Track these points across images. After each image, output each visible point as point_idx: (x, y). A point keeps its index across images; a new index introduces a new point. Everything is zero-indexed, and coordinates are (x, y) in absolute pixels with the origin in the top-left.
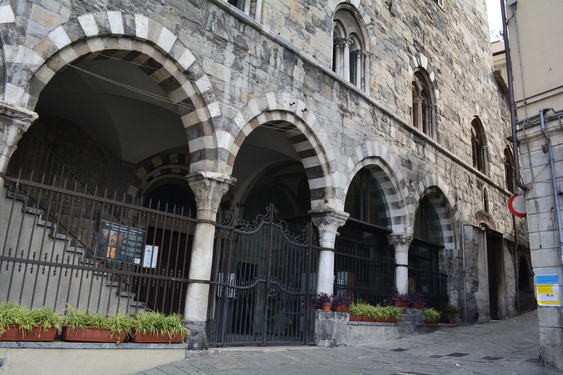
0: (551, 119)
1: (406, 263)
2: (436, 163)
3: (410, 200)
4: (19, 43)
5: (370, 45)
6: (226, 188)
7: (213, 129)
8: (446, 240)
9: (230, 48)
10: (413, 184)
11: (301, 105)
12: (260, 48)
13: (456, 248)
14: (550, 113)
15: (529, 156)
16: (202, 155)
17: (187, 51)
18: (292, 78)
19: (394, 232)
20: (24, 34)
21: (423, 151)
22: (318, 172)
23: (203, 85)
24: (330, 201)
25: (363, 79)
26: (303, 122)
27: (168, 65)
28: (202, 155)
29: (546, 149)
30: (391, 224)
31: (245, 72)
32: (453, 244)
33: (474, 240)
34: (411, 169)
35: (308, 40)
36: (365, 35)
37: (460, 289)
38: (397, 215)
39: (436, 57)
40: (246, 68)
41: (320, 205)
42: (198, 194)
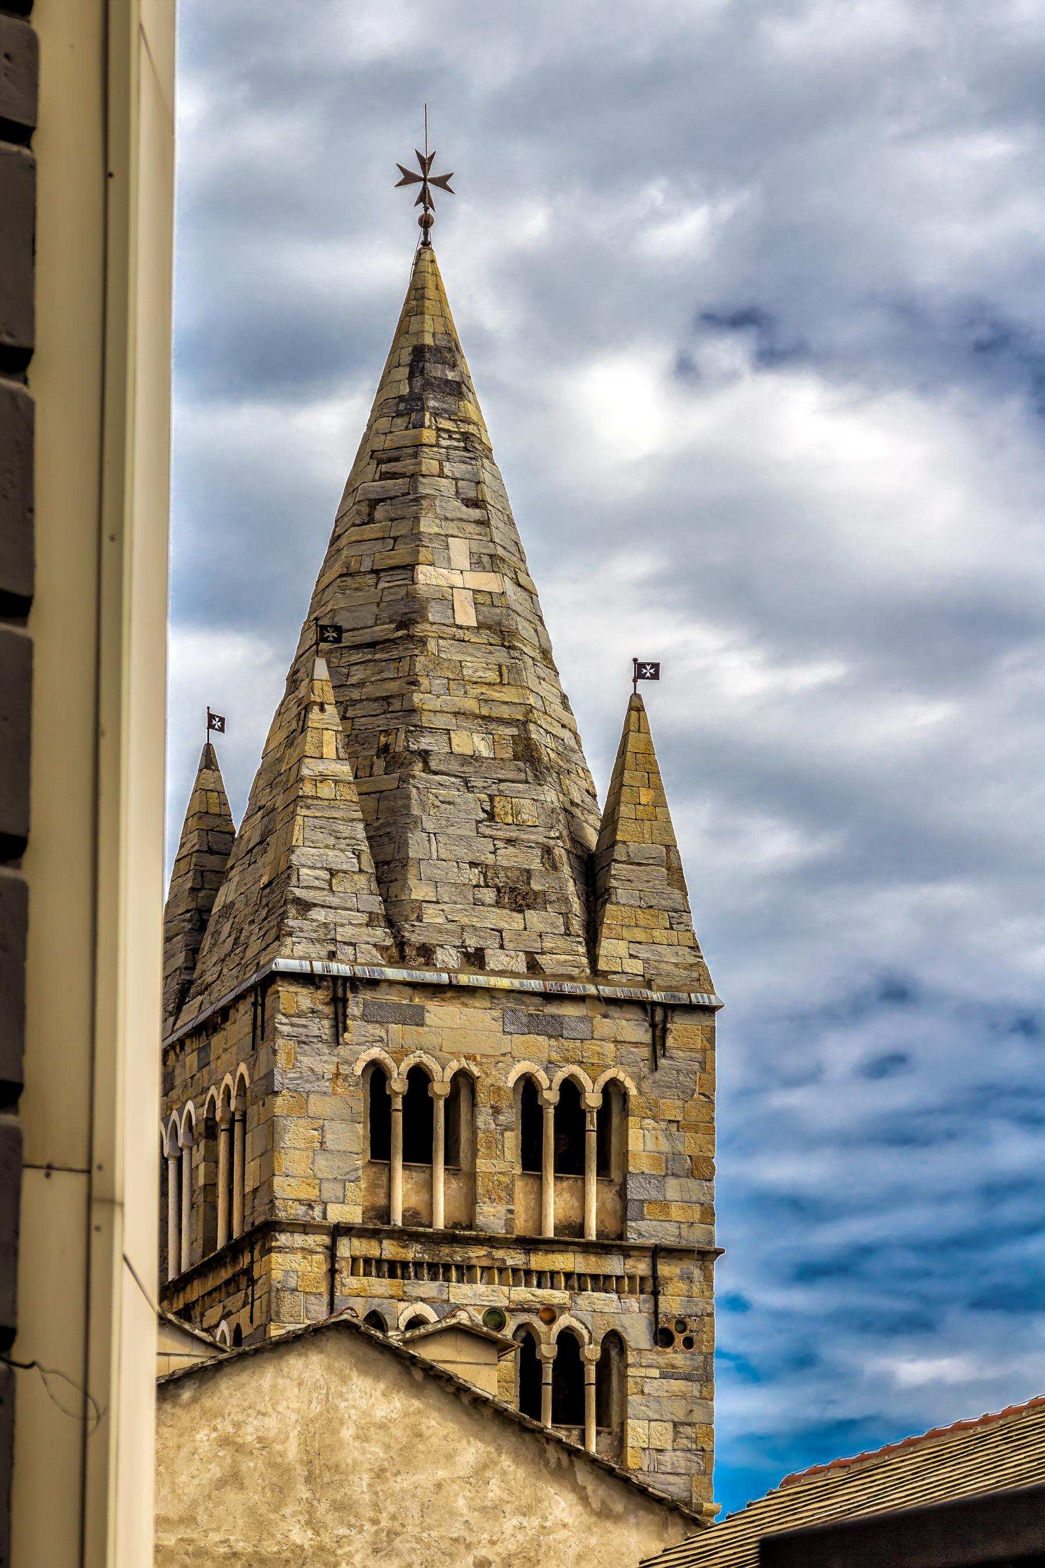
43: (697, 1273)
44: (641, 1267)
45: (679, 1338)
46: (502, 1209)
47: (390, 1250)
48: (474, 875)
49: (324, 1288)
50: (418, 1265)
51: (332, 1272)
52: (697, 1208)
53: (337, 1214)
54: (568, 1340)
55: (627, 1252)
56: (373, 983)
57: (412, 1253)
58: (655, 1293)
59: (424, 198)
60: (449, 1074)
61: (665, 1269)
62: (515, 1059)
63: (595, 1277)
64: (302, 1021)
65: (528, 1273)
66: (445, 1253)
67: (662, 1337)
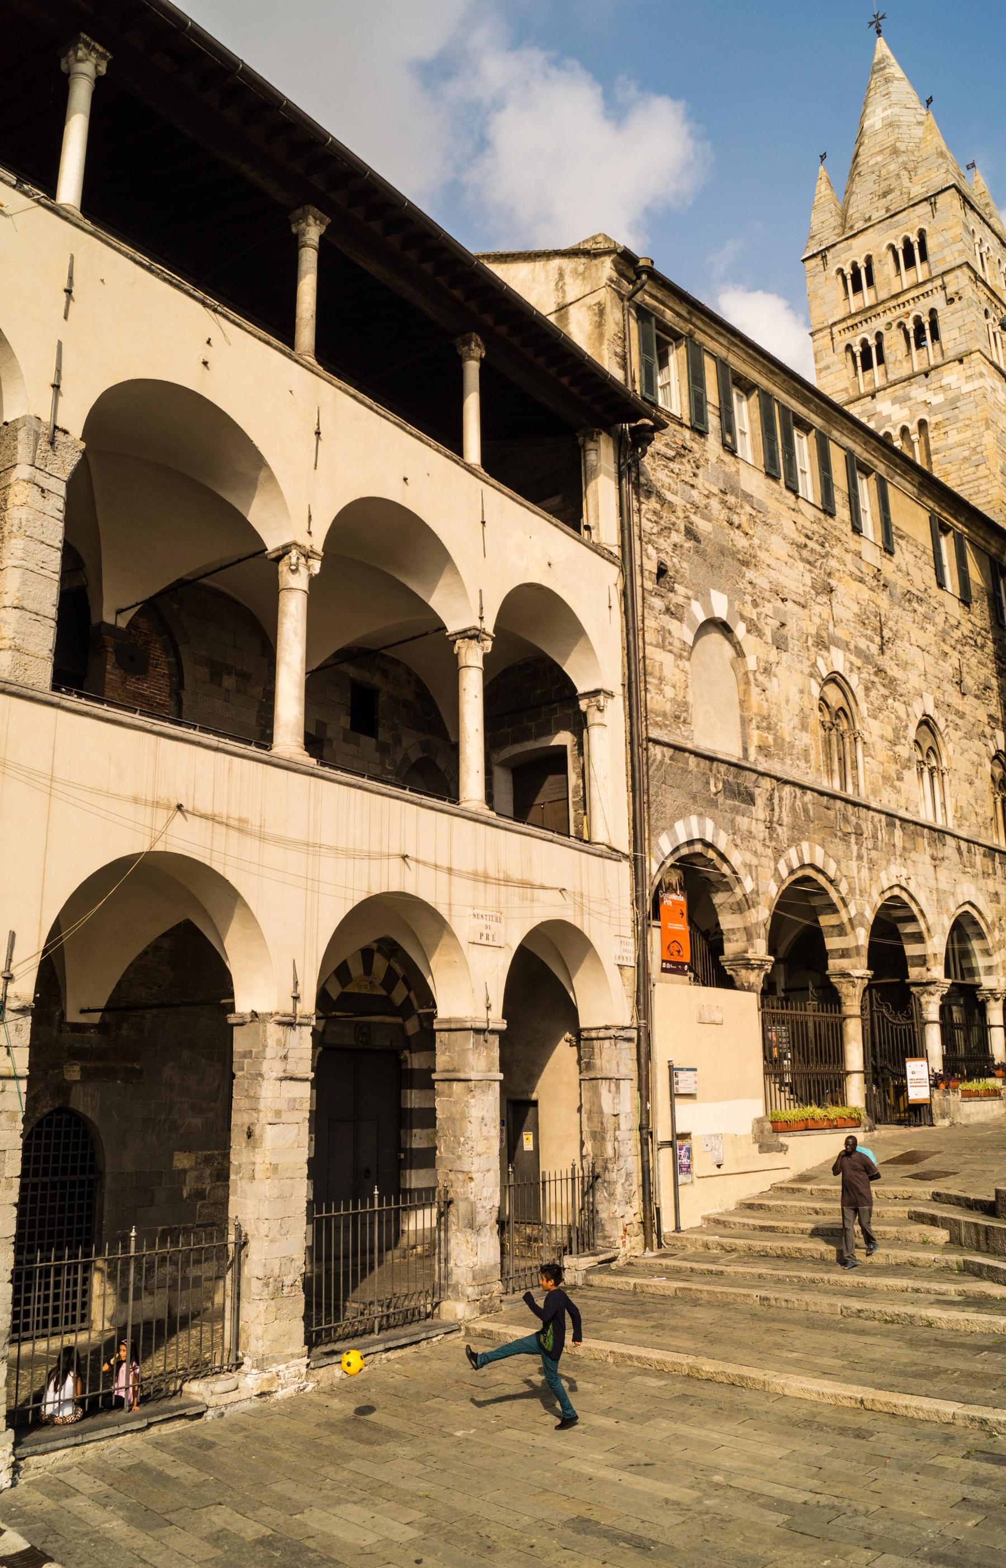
1: (1002, 1023)
4: (759, 904)
6: (866, 981)
7: (853, 928)
11: (904, 872)
12: (870, 826)
16: (844, 954)
17: (831, 860)
18: (894, 845)
20: (758, 895)
22: (919, 938)
23: (844, 887)
24: (933, 969)
26: (905, 890)
27: (821, 880)
28: (844, 954)
31: (865, 859)
34: (999, 903)
35: (899, 792)
36: (941, 745)
38: (987, 964)
40: (865, 855)
41: (920, 973)
44: (938, 282)
45: (956, 299)
46: (886, 290)
47: (850, 322)
50: (861, 322)
51: (832, 339)
54: (917, 320)
55: (930, 280)
56: (834, 245)
57: (858, 319)
61: (947, 279)
63: (923, 295)
66: (869, 314)
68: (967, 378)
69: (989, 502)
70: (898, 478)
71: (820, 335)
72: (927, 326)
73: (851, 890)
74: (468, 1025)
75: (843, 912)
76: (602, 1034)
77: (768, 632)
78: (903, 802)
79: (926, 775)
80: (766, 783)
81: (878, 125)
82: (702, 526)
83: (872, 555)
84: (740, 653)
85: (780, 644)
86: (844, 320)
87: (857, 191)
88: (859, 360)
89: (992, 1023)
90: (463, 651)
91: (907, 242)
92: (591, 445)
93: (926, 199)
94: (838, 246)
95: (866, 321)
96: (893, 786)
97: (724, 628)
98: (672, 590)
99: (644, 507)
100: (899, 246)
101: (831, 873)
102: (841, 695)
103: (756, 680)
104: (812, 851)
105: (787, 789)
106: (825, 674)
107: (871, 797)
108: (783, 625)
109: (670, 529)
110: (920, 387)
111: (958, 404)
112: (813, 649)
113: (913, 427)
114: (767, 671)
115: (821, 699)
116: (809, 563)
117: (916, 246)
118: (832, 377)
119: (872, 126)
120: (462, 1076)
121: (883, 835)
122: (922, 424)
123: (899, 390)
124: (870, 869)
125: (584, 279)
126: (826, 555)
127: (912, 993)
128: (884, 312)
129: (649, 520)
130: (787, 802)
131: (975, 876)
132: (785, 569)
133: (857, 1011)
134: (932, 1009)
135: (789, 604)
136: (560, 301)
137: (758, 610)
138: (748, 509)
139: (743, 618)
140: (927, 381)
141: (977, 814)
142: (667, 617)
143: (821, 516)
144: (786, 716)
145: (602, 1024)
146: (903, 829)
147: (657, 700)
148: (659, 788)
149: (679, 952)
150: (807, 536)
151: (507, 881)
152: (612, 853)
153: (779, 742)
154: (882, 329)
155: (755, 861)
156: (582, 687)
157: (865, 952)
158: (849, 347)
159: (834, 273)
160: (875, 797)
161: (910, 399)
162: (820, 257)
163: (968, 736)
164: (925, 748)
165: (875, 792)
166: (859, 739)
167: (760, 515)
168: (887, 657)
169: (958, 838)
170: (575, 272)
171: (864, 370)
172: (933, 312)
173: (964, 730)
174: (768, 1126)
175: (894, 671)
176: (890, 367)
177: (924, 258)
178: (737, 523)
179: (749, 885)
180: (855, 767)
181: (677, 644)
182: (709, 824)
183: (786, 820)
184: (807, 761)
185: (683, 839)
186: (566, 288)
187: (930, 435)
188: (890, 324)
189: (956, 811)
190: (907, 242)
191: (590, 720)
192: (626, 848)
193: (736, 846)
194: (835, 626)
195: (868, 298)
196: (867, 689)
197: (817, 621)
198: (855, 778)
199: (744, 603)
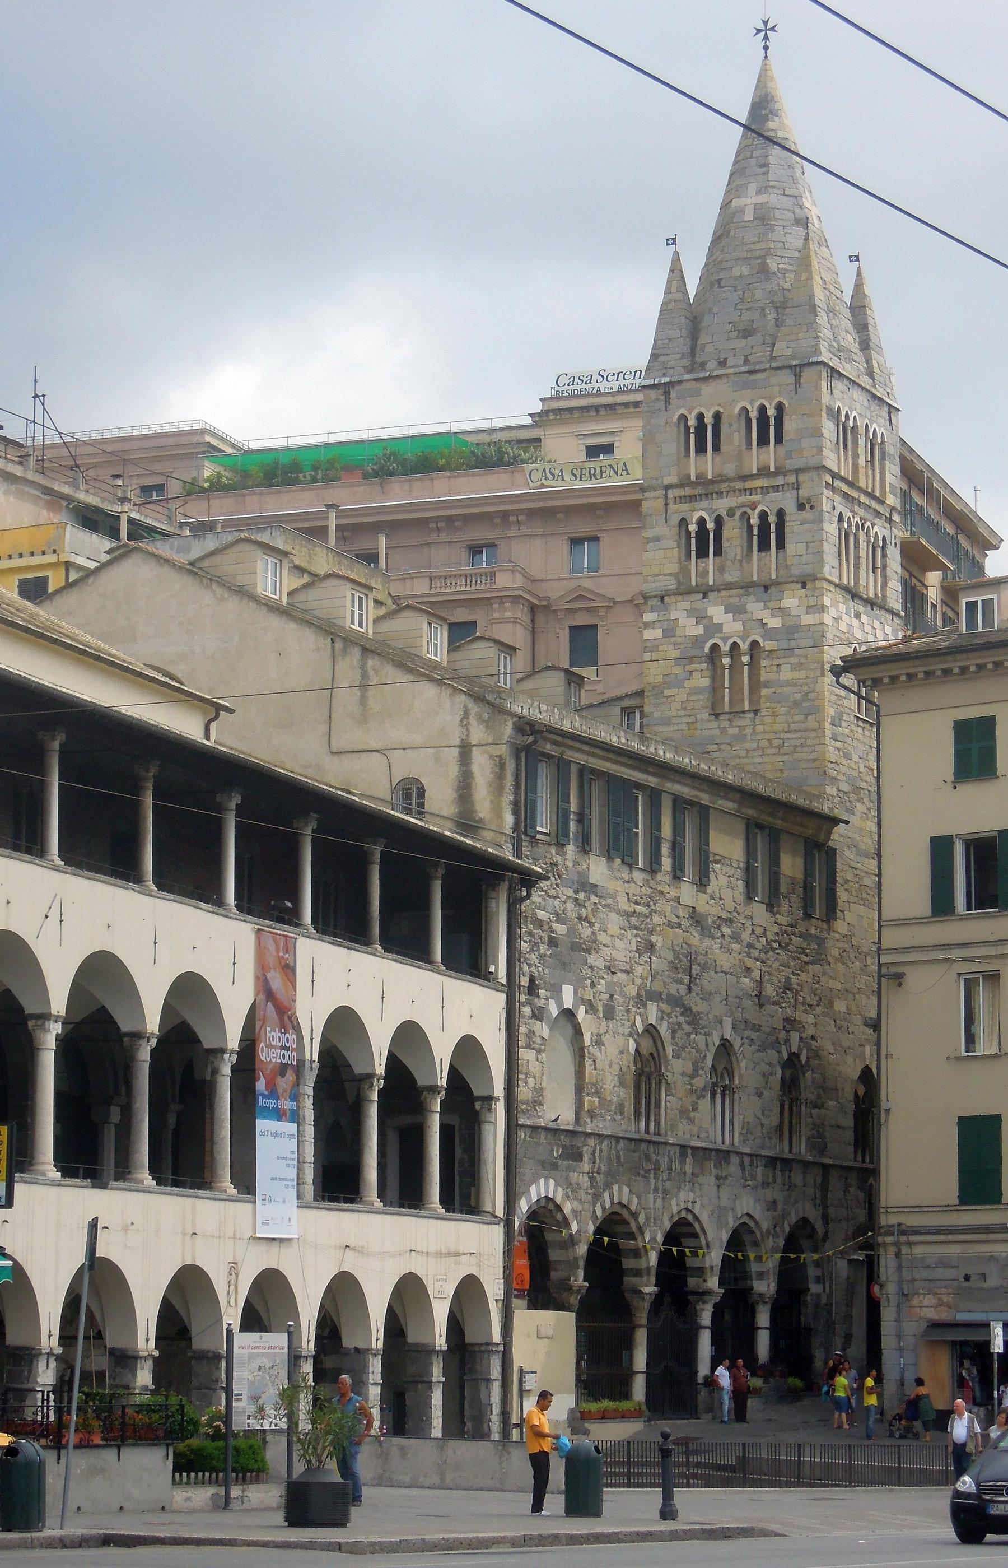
0: (904, 1233)
1: (767, 1325)
2: (804, 1186)
3: (774, 1250)
4: (580, 1241)
5: (740, 1074)
6: (653, 1297)
8: (811, 1279)
9: (652, 1176)
10: (777, 1229)
11: (691, 1195)
12: (666, 1160)
13: (824, 1291)
14: (903, 1227)
15: (886, 1258)
16: (638, 1273)
18: (685, 1173)
19: (755, 1289)
21: (789, 1177)
23: (642, 1219)
24: (709, 1280)
25: (732, 1122)
26: (691, 1212)
27: (625, 1214)
28: (638, 1273)
29: (898, 1255)
30: (751, 1280)
31: (660, 1190)
32: (821, 1286)
33: (848, 1278)
36: (735, 1064)
37: (828, 1347)
39: (810, 1019)
40: (660, 1186)
42: (635, 1303)
43: (815, 477)
44: (792, 479)
45: (808, 506)
47: (688, 491)
48: (729, 327)
49: (663, 512)
50: (700, 495)
51: (666, 504)
52: (815, 449)
53: (667, 480)
54: (764, 515)
56: (680, 382)
57: (698, 491)
58: (798, 489)
59: (766, 38)
60: (711, 414)
61: (802, 478)
62: (738, 402)
63: (773, 486)
64: (652, 404)
65: (745, 490)
67: (801, 507)
68: (809, 607)
69: (815, 760)
70: (720, 802)
71: (652, 494)
72: (773, 528)
73: (647, 1219)
74: (431, 1348)
75: (639, 1239)
76: (483, 1348)
77: (600, 1009)
78: (695, 1129)
79: (718, 1097)
80: (591, 1142)
81: (749, 215)
82: (560, 929)
83: (687, 892)
84: (578, 1032)
85: (609, 1014)
86: (680, 485)
87: (715, 310)
88: (693, 540)
89: (759, 1325)
90: (428, 1100)
91: (762, 409)
92: (492, 894)
93: (790, 367)
94: (685, 385)
95: (706, 495)
96: (689, 1119)
97: (569, 1014)
98: (538, 996)
99: (523, 930)
100: (754, 414)
101: (633, 1208)
102: (651, 1042)
103: (589, 1053)
104: (621, 1193)
105: (605, 1143)
106: (640, 1029)
107: (669, 1133)
108: (612, 996)
109: (538, 943)
110: (758, 601)
111: (796, 635)
112: (634, 1009)
113: (744, 646)
114: (599, 1042)
115: (637, 1050)
116: (636, 928)
117: (772, 421)
118: (660, 554)
119: (742, 211)
120: (425, 1379)
121: (676, 1166)
122: (754, 644)
123: (734, 597)
124: (663, 1198)
125: (487, 727)
126: (649, 916)
127: (689, 1301)
128: (728, 492)
129: (525, 942)
130: (605, 1153)
131: (755, 1188)
132: (618, 943)
133: (644, 1321)
134: (706, 1317)
135: (619, 974)
136: (464, 737)
137: (594, 990)
138: (594, 899)
139: (583, 1001)
140: (766, 596)
141: (762, 1125)
142: (533, 1021)
143: (648, 877)
144: (609, 1078)
145: (484, 1341)
146: (693, 1156)
147: (524, 1092)
148: (521, 1161)
149: (522, 1281)
150: (637, 903)
151: (449, 1254)
152: (494, 1219)
153: (603, 1102)
154: (724, 513)
155: (580, 1208)
156: (477, 1093)
157: (653, 1272)
158: (683, 522)
159: (675, 419)
160: (672, 1132)
161: (746, 612)
162: (661, 391)
163: (763, 1048)
164: (720, 1068)
165: (673, 1127)
166: (664, 1080)
167: (601, 900)
168: (693, 994)
169: (742, 1153)
170: (479, 717)
171: (698, 557)
172: (781, 514)
173: (759, 1043)
174: (579, 1414)
175: (698, 1006)
176: (728, 563)
177: (779, 439)
178: (584, 916)
179: (574, 1227)
180: (658, 1105)
181: (538, 1040)
182: (552, 1182)
183: (603, 1168)
184: (622, 1114)
185: (534, 1199)
186: (470, 728)
187: (763, 663)
188: (731, 509)
189: (743, 1128)
190: (762, 409)
191: (482, 1117)
192: (500, 1212)
193: (568, 1197)
194: (652, 981)
195: (708, 465)
196: (674, 1032)
197: (638, 981)
198: (658, 1115)
199: (584, 988)
